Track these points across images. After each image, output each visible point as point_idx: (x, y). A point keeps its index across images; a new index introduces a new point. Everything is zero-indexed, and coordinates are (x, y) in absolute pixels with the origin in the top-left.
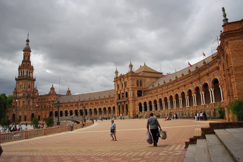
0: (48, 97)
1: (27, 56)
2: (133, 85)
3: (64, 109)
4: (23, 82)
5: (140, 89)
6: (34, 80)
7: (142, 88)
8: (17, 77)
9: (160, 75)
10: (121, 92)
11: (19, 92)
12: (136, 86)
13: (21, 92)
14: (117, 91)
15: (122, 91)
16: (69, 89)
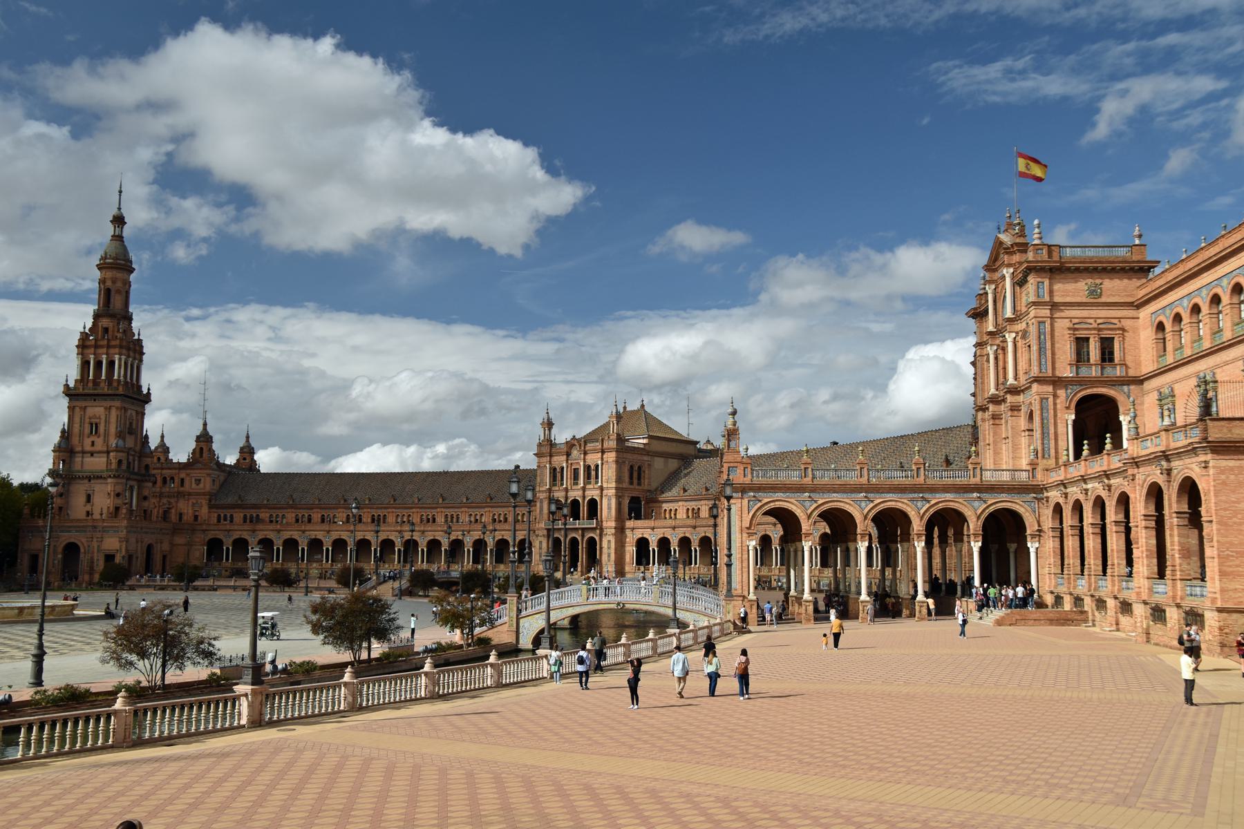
0: (183, 475)
1: (118, 292)
2: (619, 480)
3: (279, 531)
4: (109, 409)
5: (635, 494)
6: (147, 399)
7: (643, 491)
8: (72, 384)
9: (690, 450)
10: (567, 498)
11: (88, 448)
12: (625, 485)
13: (99, 452)
14: (550, 490)
15: (575, 494)
16: (248, 437)
